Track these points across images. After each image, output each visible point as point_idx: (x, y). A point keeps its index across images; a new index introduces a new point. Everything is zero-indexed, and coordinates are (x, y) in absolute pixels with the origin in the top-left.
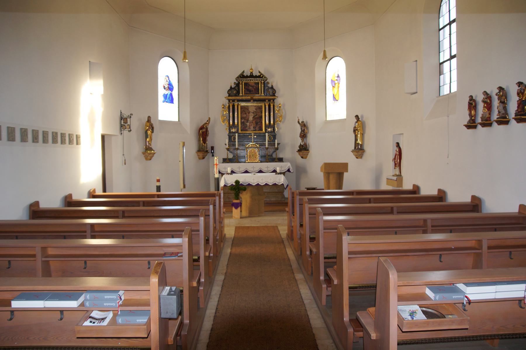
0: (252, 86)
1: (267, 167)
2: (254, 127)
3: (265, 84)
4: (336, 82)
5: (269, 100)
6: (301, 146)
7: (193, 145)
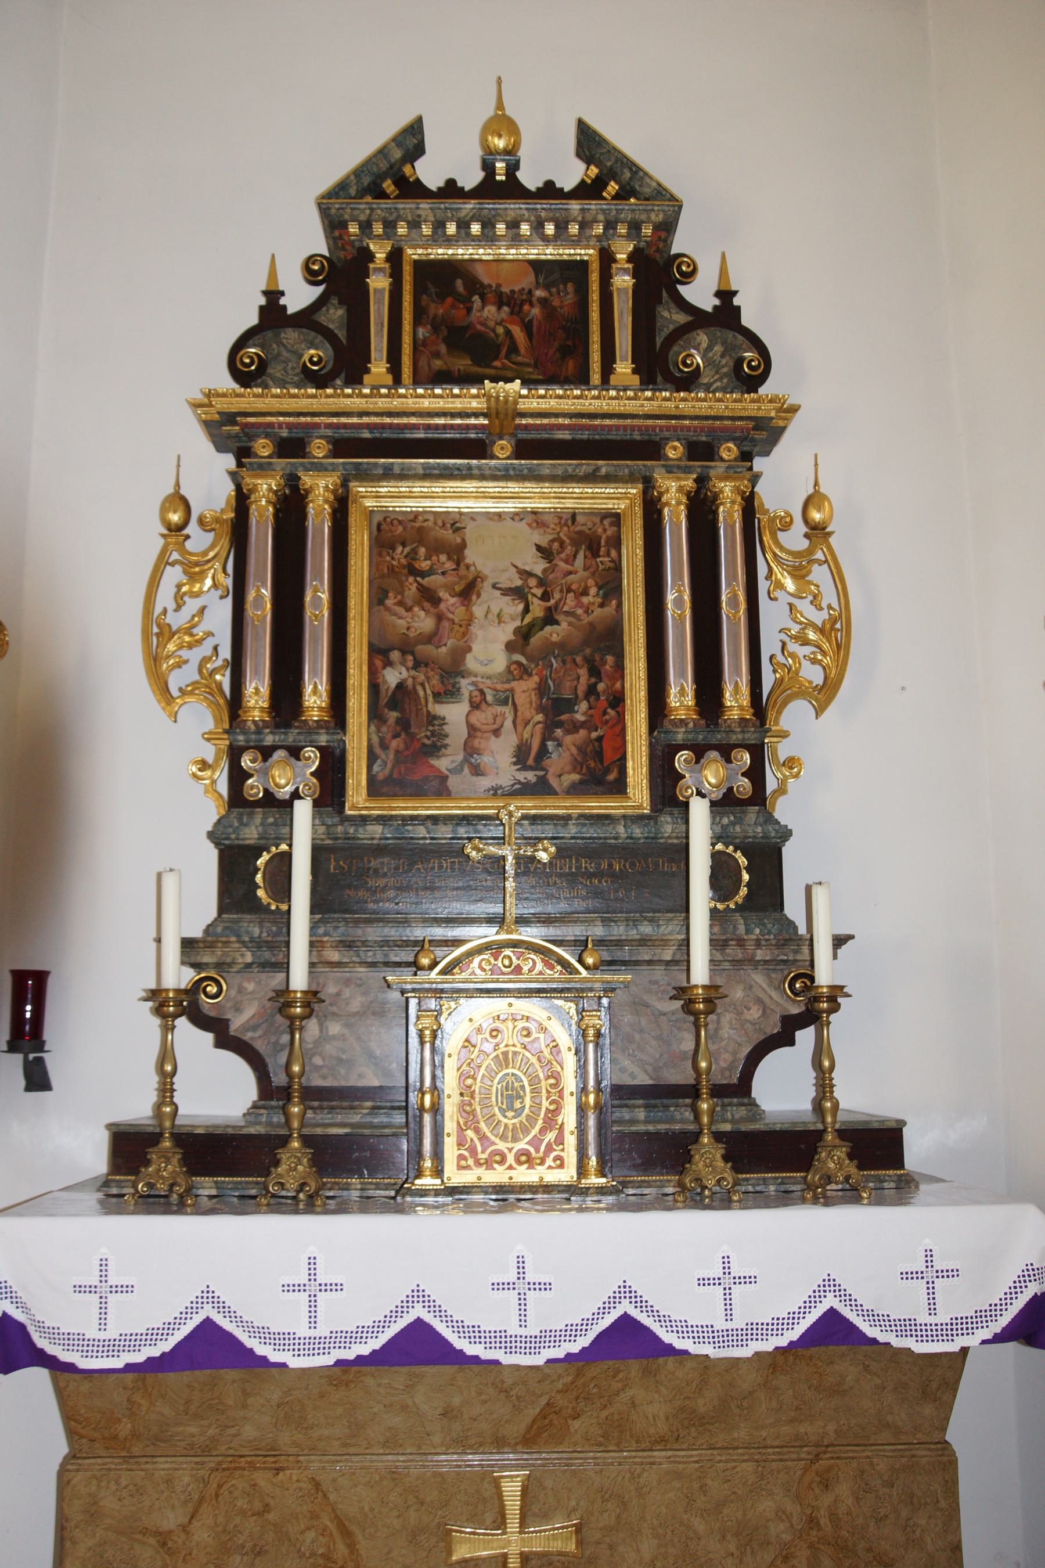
0: (501, 300)
2: (521, 757)
3: (660, 272)
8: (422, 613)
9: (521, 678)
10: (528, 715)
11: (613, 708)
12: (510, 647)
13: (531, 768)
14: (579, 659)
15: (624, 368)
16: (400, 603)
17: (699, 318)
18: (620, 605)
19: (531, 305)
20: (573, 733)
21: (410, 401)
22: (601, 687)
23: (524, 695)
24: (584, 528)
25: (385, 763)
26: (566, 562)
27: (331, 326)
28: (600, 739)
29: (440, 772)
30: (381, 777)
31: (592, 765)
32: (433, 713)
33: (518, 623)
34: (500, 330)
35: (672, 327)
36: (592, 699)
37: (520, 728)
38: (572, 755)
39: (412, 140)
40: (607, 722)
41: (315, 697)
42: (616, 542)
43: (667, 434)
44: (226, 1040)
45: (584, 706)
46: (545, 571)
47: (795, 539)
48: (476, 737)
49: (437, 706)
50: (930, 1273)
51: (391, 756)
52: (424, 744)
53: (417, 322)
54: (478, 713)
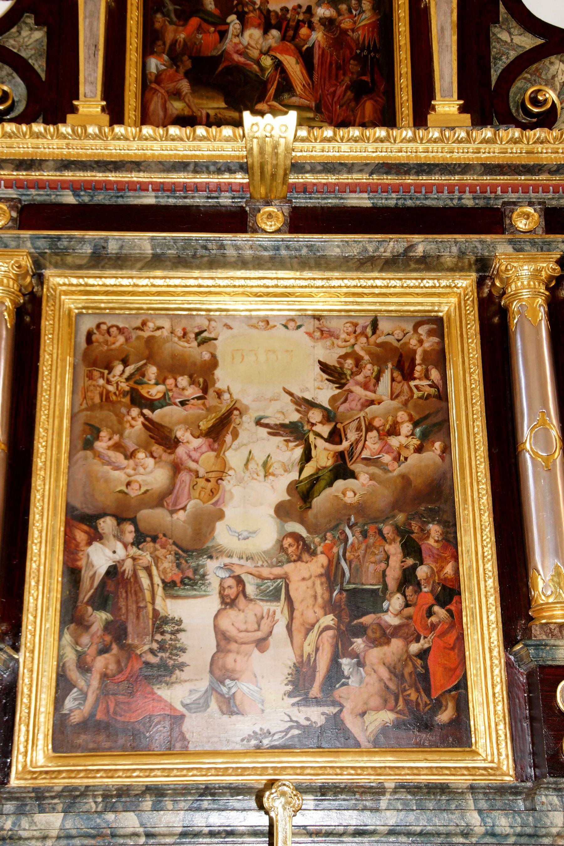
8: (150, 462)
9: (299, 559)
10: (310, 616)
11: (443, 606)
12: (282, 511)
13: (318, 702)
14: (387, 530)
15: (447, 105)
16: (118, 447)
18: (447, 449)
19: (311, 27)
20: (381, 645)
21: (135, 144)
22: (422, 572)
23: (304, 585)
24: (389, 339)
25: (84, 695)
26: (365, 386)
27: (23, 54)
28: (423, 654)
29: (172, 708)
30: (76, 718)
31: (413, 696)
32: (162, 613)
33: (294, 476)
34: (267, 62)
35: (513, 55)
36: (409, 591)
37: (298, 637)
38: (381, 680)
40: (433, 627)
42: (439, 358)
43: (513, 197)
45: (396, 602)
46: (333, 399)
48: (229, 651)
49: (169, 602)
51: (95, 682)
52: (147, 664)
53: (148, 49)
54: (232, 613)
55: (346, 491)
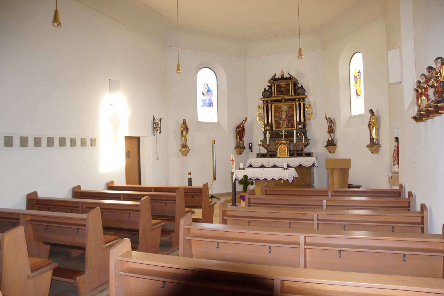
0: (283, 88)
1: (294, 162)
2: (286, 125)
3: (295, 85)
4: (358, 77)
5: (299, 99)
6: (329, 141)
7: (231, 140)
17: (299, 88)
39: (275, 75)
41: (270, 121)
44: (264, 148)
47: (308, 106)
50: (307, 162)
55: (289, 115)
